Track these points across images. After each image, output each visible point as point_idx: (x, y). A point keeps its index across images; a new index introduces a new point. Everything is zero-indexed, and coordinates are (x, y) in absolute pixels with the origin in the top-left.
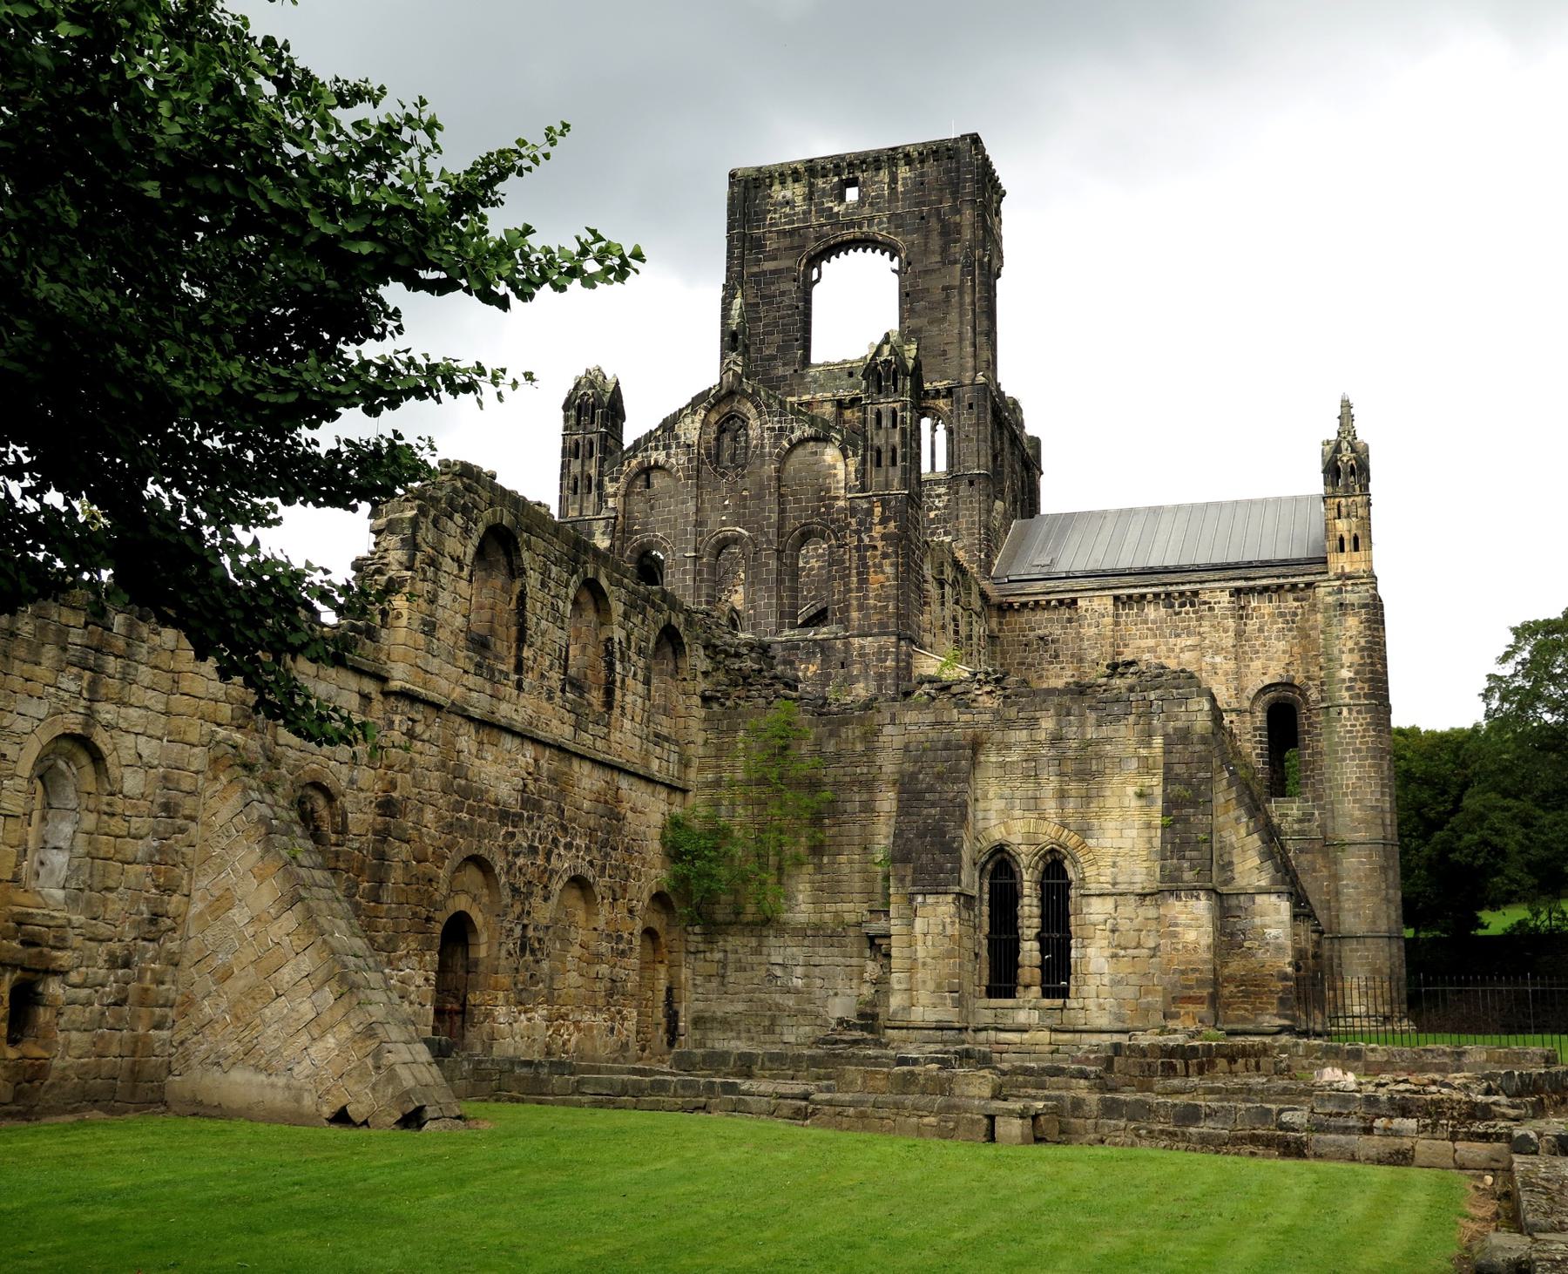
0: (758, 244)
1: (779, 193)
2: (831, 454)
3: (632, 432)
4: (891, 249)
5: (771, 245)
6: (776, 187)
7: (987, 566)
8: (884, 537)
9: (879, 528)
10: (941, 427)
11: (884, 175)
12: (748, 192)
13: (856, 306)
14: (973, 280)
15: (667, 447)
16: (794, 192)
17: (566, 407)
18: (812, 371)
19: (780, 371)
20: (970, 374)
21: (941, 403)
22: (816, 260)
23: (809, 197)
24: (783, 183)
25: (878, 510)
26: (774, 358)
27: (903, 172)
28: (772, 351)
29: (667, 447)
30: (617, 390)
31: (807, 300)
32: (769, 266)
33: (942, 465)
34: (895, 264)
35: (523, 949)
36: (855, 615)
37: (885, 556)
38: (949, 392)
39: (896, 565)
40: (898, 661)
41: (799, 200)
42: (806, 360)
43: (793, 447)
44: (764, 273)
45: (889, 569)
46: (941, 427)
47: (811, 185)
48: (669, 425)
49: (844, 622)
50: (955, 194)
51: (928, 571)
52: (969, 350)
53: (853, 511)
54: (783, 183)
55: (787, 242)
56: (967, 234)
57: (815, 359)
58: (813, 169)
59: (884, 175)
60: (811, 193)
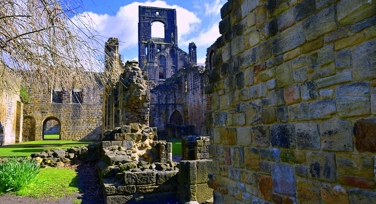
4: (164, 23)
5: (146, 18)
6: (146, 10)
11: (163, 12)
13: (158, 30)
15: (164, 53)
19: (147, 38)
22: (152, 22)
26: (146, 36)
27: (165, 12)
28: (146, 34)
29: (164, 53)
32: (145, 21)
41: (150, 13)
44: (145, 22)
55: (148, 18)
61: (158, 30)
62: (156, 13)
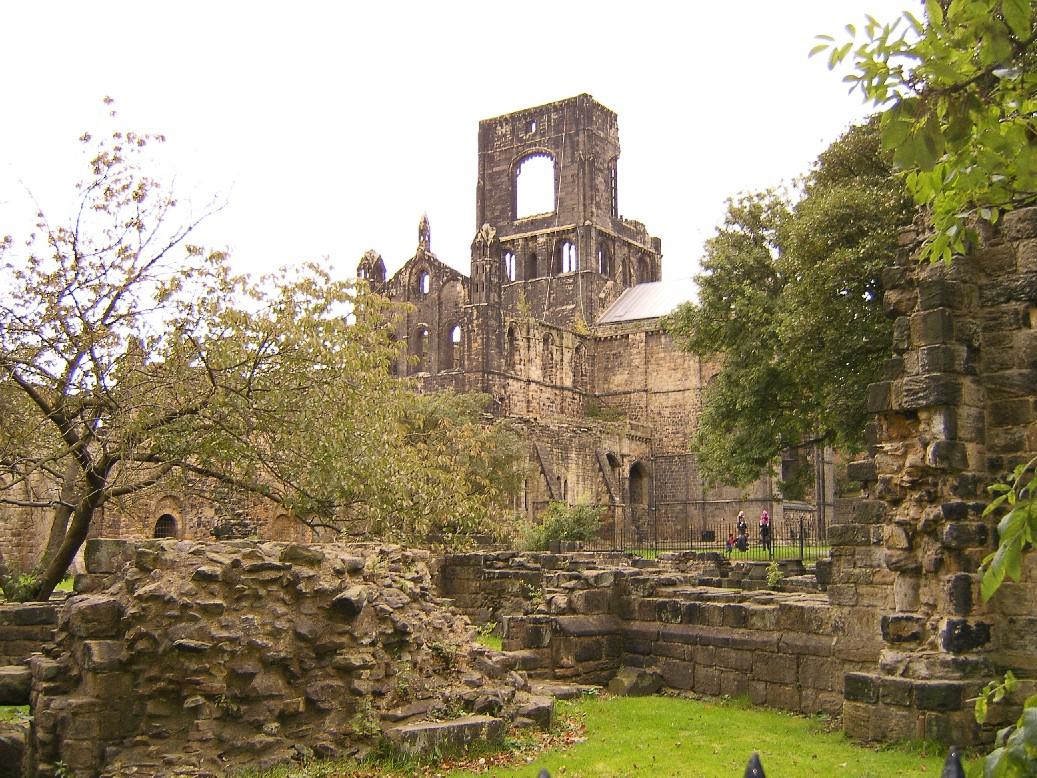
0: (491, 157)
1: (500, 131)
2: (459, 287)
3: (389, 276)
5: (497, 159)
7: (591, 320)
8: (477, 325)
9: (476, 322)
10: (573, 247)
11: (545, 118)
12: (488, 131)
13: (537, 188)
14: (584, 174)
16: (506, 129)
17: (358, 270)
18: (516, 223)
20: (582, 220)
21: (571, 235)
23: (513, 132)
24: (502, 126)
25: (475, 313)
27: (554, 116)
30: (380, 259)
31: (514, 186)
33: (573, 269)
34: (552, 163)
35: (199, 525)
36: (466, 363)
37: (478, 334)
38: (574, 230)
39: (482, 339)
40: (483, 383)
42: (514, 217)
43: (444, 284)
45: (480, 341)
46: (573, 247)
47: (513, 126)
48: (397, 276)
49: (462, 366)
50: (577, 125)
51: (519, 335)
52: (581, 208)
53: (465, 313)
54: (502, 126)
56: (581, 146)
57: (520, 215)
58: (513, 118)
59: (545, 118)
60: (514, 129)
61: (537, 188)
62: (528, 129)
